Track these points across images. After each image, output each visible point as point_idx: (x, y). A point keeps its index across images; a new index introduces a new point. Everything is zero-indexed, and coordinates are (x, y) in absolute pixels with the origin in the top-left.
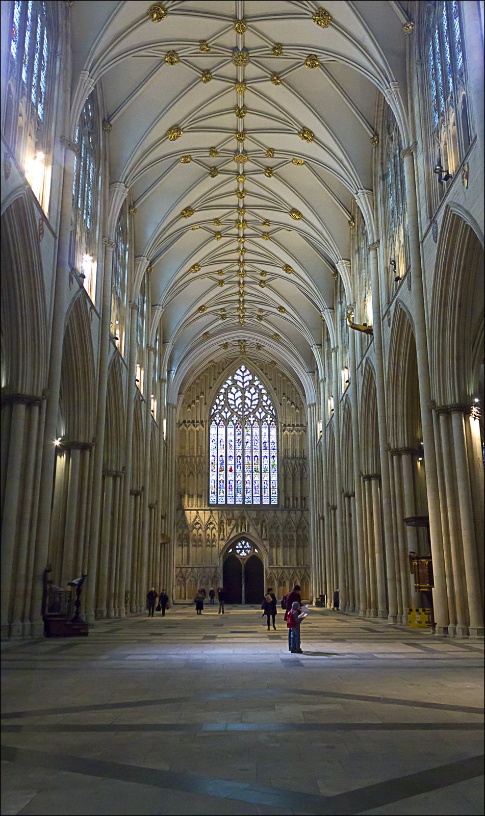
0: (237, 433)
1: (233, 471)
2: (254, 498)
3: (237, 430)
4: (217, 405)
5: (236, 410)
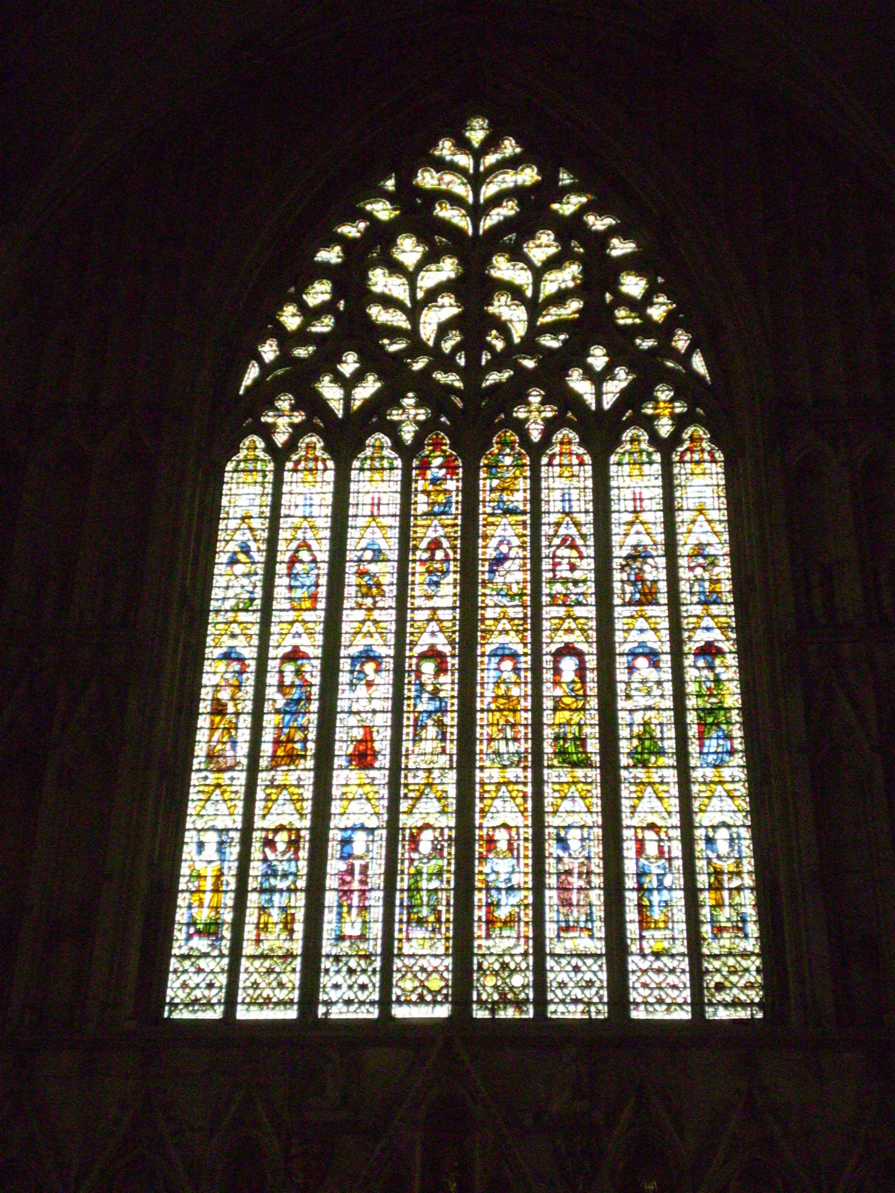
0: (421, 504)
1: (384, 761)
2: (556, 972)
3: (421, 485)
4: (287, 340)
5: (419, 365)
